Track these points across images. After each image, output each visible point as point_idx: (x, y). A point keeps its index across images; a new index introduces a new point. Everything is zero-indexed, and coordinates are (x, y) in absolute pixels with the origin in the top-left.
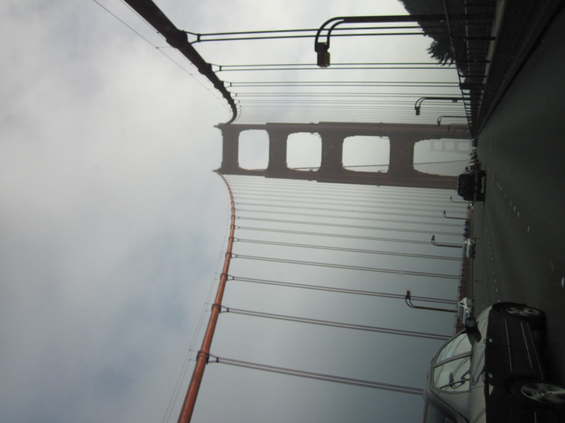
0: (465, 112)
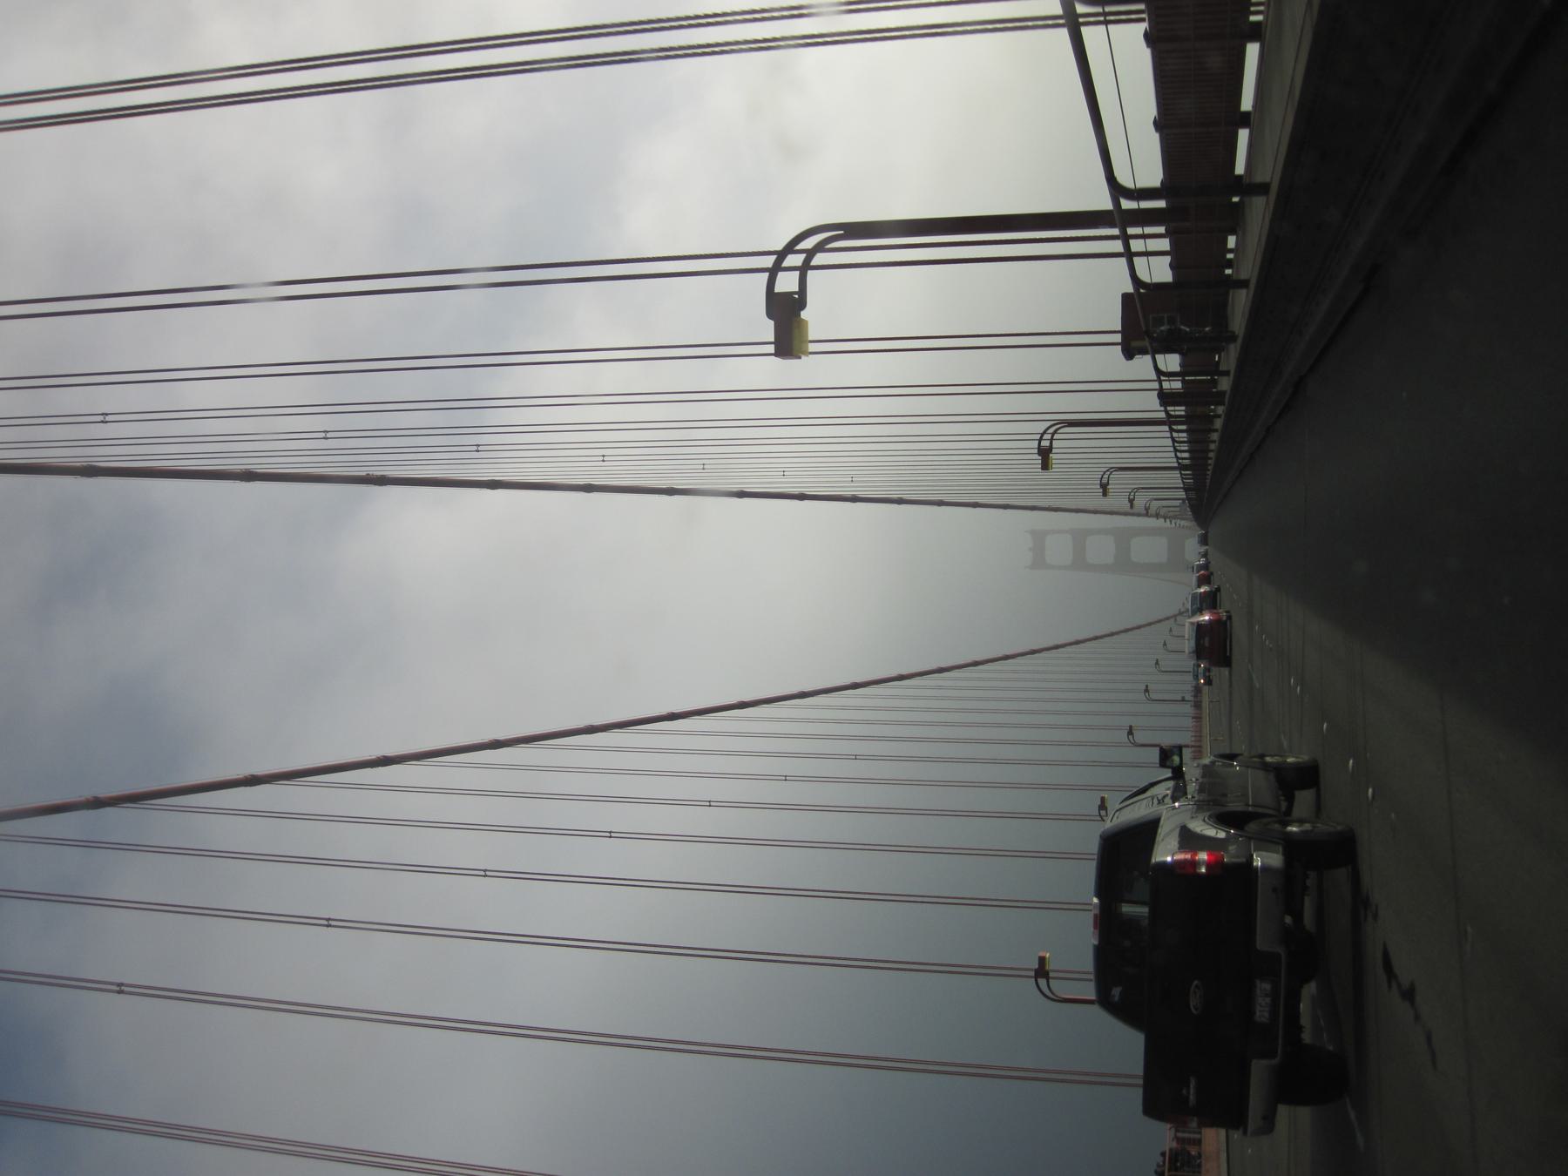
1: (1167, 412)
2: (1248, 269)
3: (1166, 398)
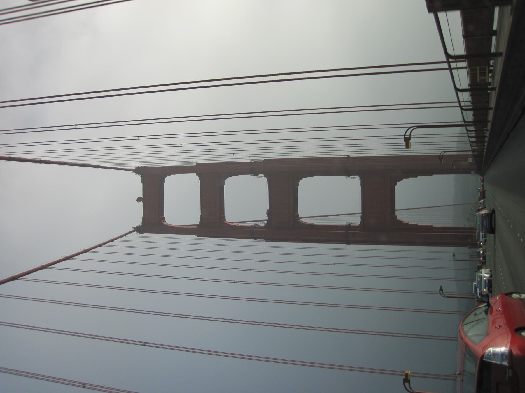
2: (497, 85)
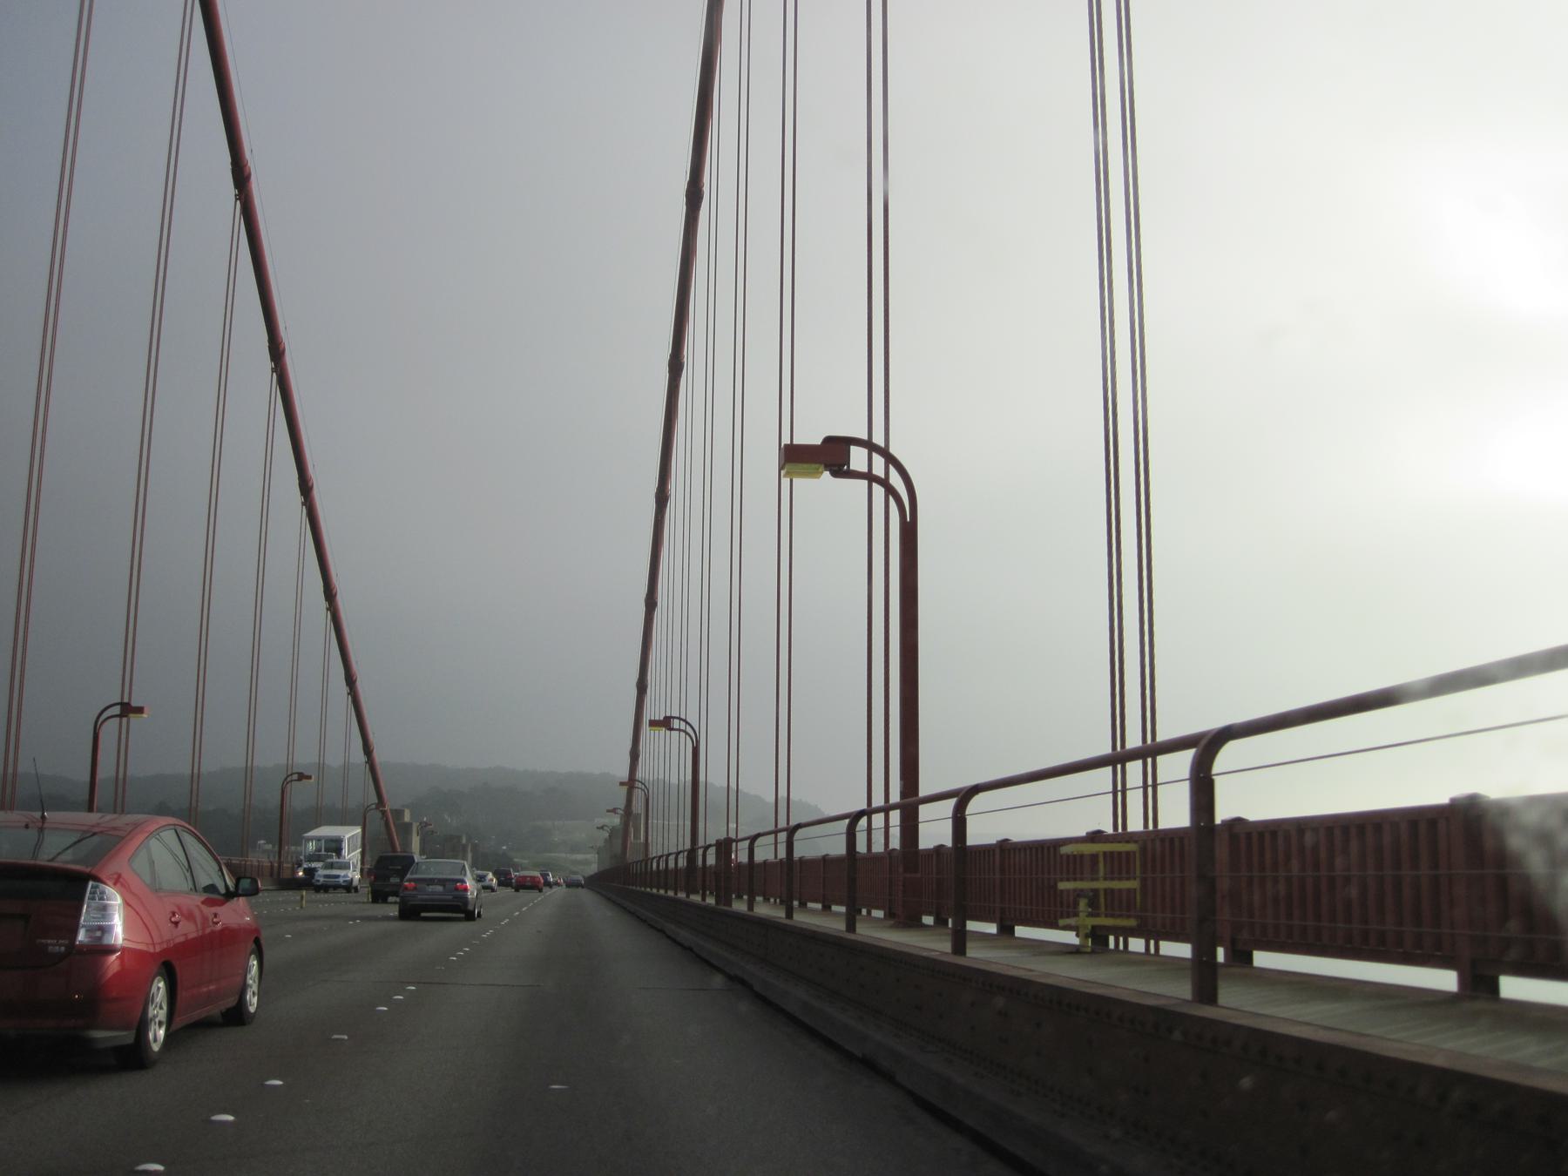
0: (674, 850)
1: (706, 848)
3: (724, 847)
